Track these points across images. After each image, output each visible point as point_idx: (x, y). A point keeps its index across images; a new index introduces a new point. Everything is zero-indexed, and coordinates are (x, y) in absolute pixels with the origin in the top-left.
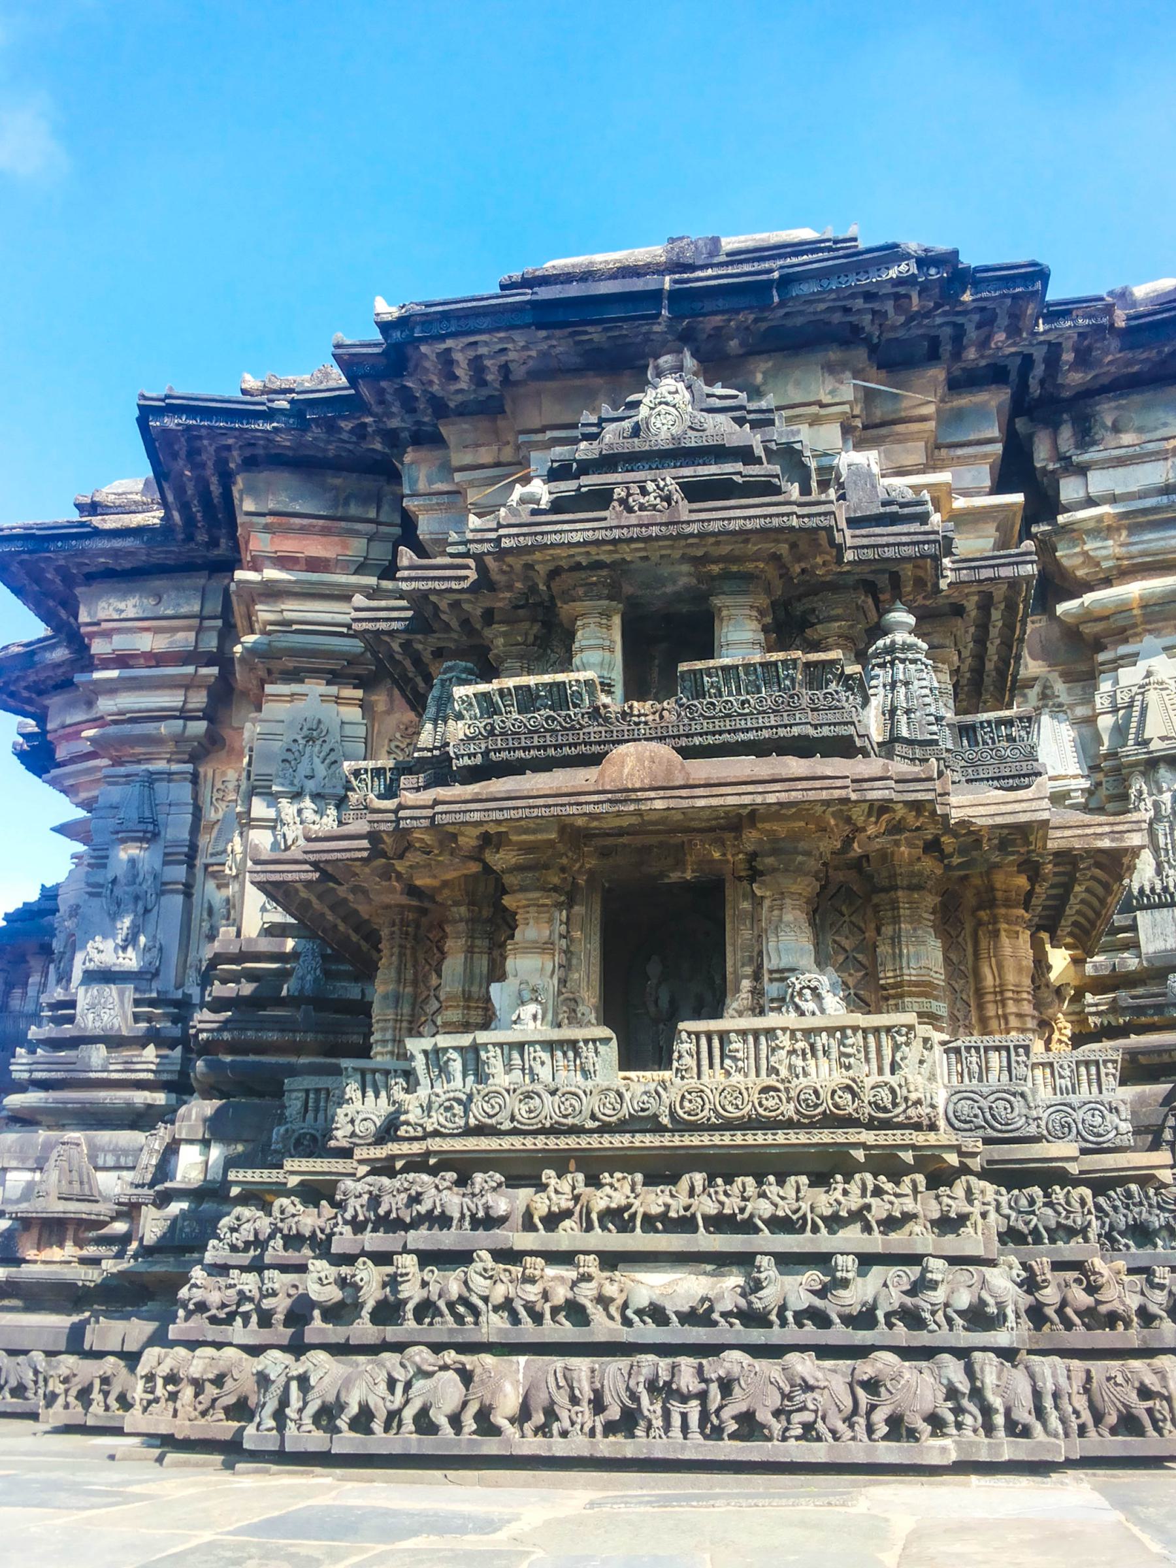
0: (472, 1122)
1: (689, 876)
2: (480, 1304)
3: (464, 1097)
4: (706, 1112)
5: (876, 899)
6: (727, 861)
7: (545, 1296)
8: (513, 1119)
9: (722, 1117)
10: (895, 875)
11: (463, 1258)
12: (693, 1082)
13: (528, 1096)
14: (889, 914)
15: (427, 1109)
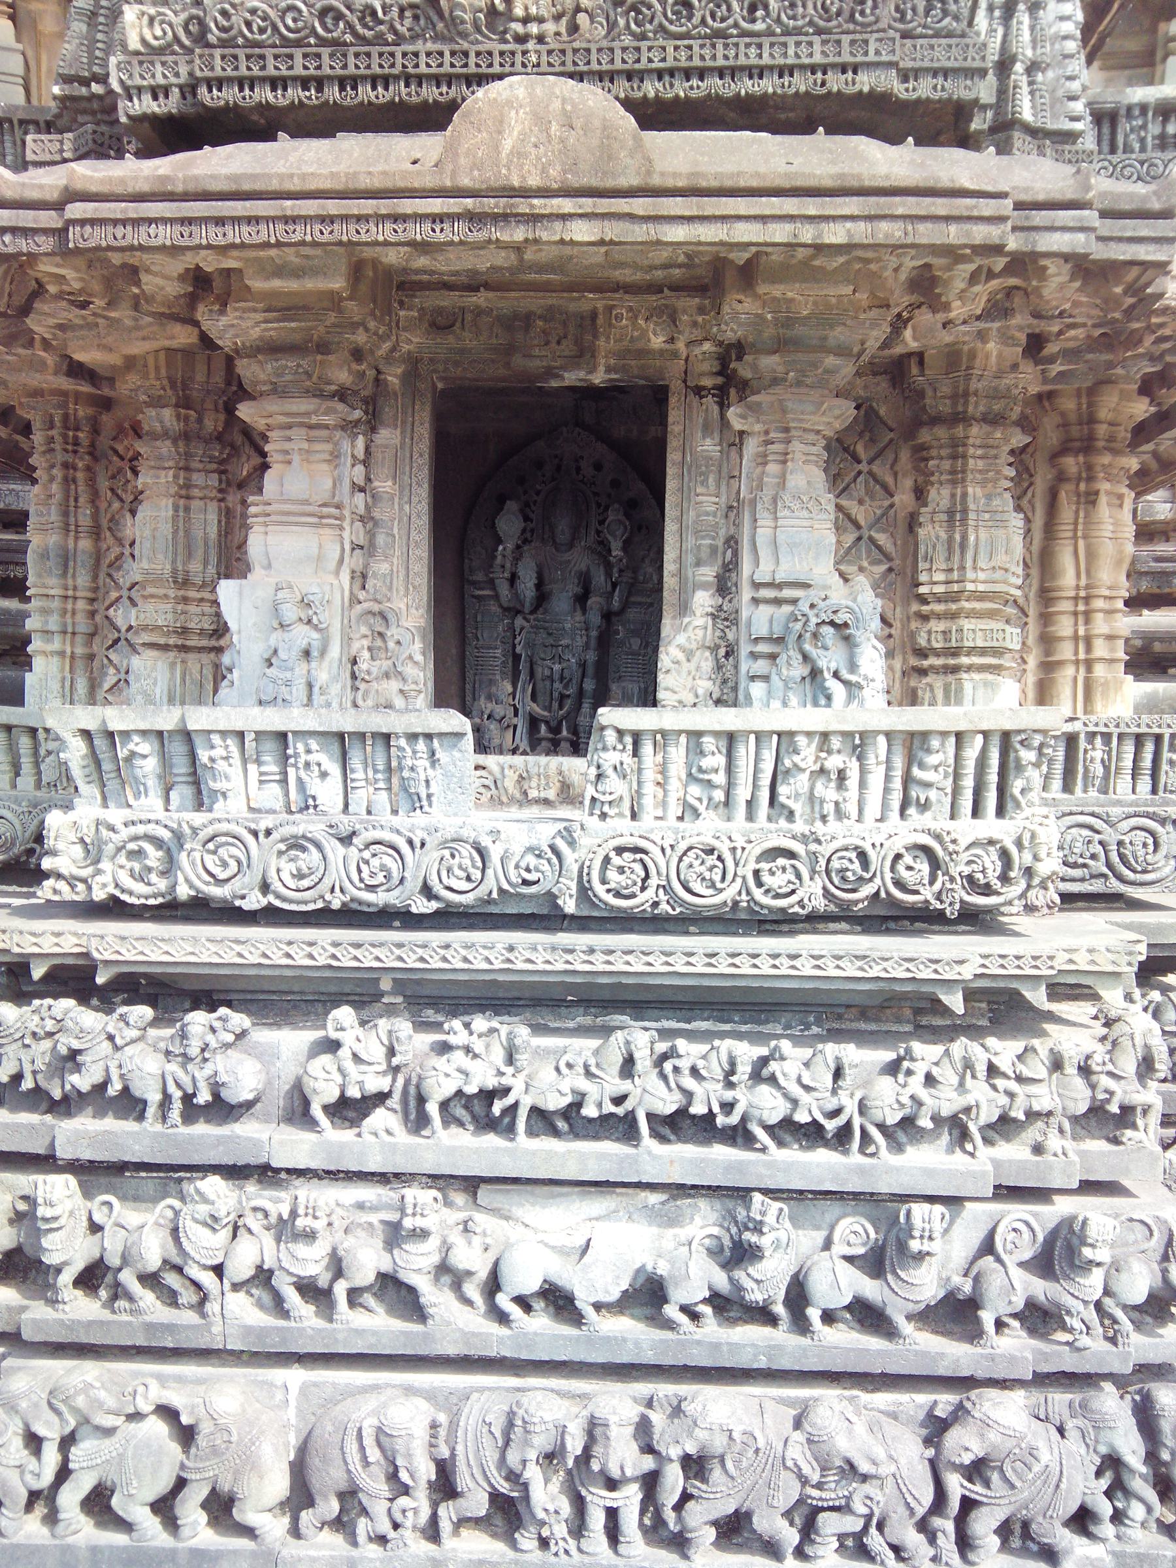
0: (183, 892)
1: (598, 378)
2: (208, 1279)
3: (166, 835)
4: (650, 894)
5: (924, 436)
6: (675, 354)
7: (337, 1267)
8: (265, 888)
9: (683, 903)
10: (966, 394)
11: (172, 1174)
12: (621, 828)
13: (296, 844)
14: (946, 465)
15: (93, 852)
